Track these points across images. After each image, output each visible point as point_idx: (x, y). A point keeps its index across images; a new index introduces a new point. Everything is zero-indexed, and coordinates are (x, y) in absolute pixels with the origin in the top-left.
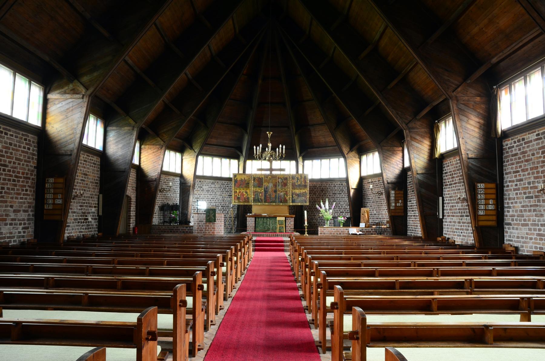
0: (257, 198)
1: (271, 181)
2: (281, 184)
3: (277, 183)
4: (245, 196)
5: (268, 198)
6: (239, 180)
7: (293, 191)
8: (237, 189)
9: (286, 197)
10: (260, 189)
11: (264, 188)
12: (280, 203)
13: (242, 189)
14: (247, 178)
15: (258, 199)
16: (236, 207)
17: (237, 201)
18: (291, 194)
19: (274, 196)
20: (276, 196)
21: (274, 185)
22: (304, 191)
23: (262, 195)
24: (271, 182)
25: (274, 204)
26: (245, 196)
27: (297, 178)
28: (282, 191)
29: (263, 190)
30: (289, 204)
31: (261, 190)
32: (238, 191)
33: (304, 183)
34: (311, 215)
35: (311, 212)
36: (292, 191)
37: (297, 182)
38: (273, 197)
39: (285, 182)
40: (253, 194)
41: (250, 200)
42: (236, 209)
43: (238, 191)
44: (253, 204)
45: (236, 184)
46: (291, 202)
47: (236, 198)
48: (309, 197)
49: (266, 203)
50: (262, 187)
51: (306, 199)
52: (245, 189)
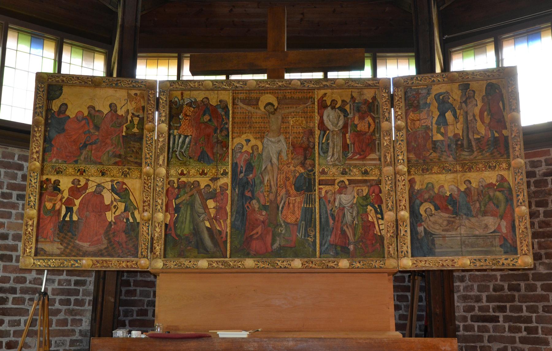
0: (186, 229)
1: (275, 122)
2: (338, 140)
3: (311, 133)
4: (110, 216)
5: (259, 229)
6: (79, 118)
7: (417, 178)
8: (59, 172)
9: (372, 217)
10: (211, 171)
11: (235, 166)
12: (337, 255)
13: (93, 169)
14: (131, 107)
15: (196, 232)
16: (86, 293)
17: (54, 247)
18: (405, 201)
19: (298, 214)
20: (308, 215)
21: (294, 147)
22: (491, 177)
23: (220, 209)
24: (279, 134)
25: (297, 263)
26: (110, 216)
27: (437, 97)
28: (345, 179)
29: (227, 180)
30: (391, 263)
31: (214, 179)
32: (65, 183)
33: (490, 127)
34: (512, 340)
35: (507, 319)
36: (412, 182)
37: (442, 121)
38: (291, 219)
39: (362, 126)
40: (161, 200)
41: (143, 247)
42: (88, 307)
43: (65, 183)
44: (159, 264)
45: (59, 140)
46: (407, 247)
47: (50, 228)
48: (532, 215)
49: (248, 255)
50: (223, 158)
51: (513, 227)
52: (115, 170)
